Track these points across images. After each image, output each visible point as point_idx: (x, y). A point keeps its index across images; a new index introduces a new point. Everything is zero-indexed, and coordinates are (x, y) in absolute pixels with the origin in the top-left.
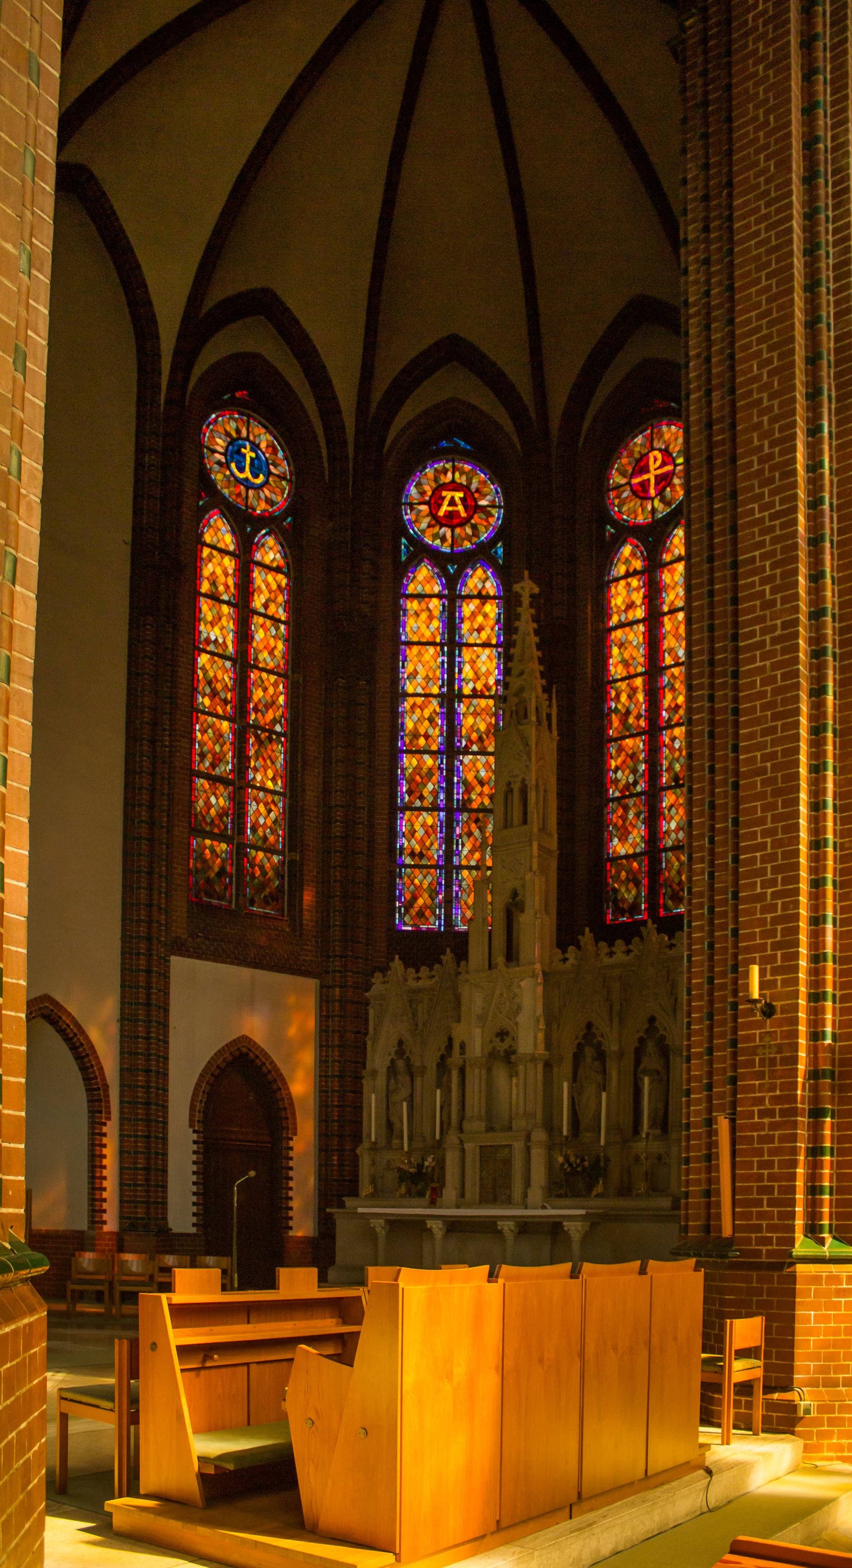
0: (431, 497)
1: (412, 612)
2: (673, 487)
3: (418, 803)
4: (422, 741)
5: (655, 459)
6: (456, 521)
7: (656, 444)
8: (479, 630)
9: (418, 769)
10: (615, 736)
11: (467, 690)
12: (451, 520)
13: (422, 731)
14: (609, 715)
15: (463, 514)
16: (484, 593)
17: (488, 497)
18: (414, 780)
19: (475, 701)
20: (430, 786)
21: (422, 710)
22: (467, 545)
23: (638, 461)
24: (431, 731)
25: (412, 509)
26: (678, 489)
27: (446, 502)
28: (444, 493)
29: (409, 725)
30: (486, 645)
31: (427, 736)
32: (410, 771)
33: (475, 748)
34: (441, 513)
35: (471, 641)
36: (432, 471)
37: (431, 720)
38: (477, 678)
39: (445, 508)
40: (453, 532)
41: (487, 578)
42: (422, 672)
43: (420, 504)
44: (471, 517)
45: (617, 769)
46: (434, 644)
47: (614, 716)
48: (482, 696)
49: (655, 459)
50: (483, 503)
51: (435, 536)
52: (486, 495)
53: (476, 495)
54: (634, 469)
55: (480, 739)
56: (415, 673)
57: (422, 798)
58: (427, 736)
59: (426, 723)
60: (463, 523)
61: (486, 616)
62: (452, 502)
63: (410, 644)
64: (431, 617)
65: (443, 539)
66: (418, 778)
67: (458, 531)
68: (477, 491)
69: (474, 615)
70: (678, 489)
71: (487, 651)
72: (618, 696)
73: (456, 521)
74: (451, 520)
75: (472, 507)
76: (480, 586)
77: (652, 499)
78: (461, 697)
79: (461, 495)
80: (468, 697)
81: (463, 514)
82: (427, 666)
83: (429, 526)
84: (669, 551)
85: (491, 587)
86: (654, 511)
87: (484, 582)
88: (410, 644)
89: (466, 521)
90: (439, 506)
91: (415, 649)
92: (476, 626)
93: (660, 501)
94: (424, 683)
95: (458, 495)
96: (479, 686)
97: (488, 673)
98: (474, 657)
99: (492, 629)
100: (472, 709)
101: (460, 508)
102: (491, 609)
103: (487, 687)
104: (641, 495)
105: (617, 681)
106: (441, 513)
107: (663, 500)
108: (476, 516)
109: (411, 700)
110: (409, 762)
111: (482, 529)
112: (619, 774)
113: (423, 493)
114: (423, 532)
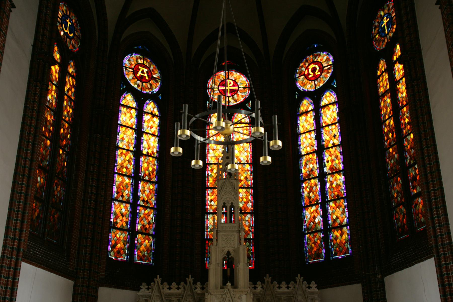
0: (134, 67)
1: (123, 112)
2: (238, 95)
3: (121, 198)
4: (124, 170)
5: (230, 83)
6: (144, 80)
7: (230, 77)
8: (151, 127)
9: (121, 183)
10: (211, 186)
11: (145, 152)
12: (141, 79)
13: (125, 165)
14: (208, 177)
15: (147, 78)
16: (153, 113)
17: (157, 74)
18: (120, 187)
19: (148, 158)
20: (127, 192)
21: (126, 156)
22: (148, 91)
23: (222, 81)
24: (129, 166)
25: (126, 69)
26: (240, 96)
27: (140, 71)
28: (140, 67)
29: (119, 161)
30: (153, 135)
31: (127, 168)
32: (118, 183)
33: (147, 178)
34: (138, 75)
35: (147, 131)
36: (135, 57)
37: (129, 161)
38: (149, 148)
39: (139, 74)
40: (142, 84)
41: (155, 108)
42: (126, 140)
43: (129, 68)
44: (150, 81)
45: (211, 201)
46: (132, 128)
47: (210, 178)
48: (151, 156)
49: (230, 83)
50: (155, 76)
51: (135, 83)
52: (156, 74)
53: (152, 72)
54: (220, 83)
55: (149, 174)
56: (123, 139)
57: (123, 196)
58: (127, 168)
59: (127, 162)
60: (147, 82)
61: (154, 122)
62: (143, 72)
63: (122, 126)
64: (131, 117)
65: (138, 86)
66: (121, 187)
67: (144, 84)
68: (153, 71)
69: (149, 121)
70: (240, 96)
71: (153, 138)
72: (212, 170)
73: (144, 80)
74: (141, 79)
75: (151, 78)
76: (152, 110)
77: (229, 97)
78: (142, 155)
79: (147, 70)
80: (145, 155)
81: (147, 78)
82: (128, 137)
83: (133, 78)
84: (236, 118)
85: (156, 112)
86: (229, 102)
87: (154, 109)
88: (122, 126)
89: (148, 81)
90: (137, 73)
91: (124, 129)
92: (150, 126)
93: (232, 98)
94: (127, 144)
95: (145, 70)
96: (150, 151)
97: (154, 147)
98: (148, 138)
99: (156, 129)
100: (146, 161)
101: (146, 75)
102: (156, 120)
103: (153, 152)
104: (223, 94)
105: (212, 164)
106: (138, 75)
107: (233, 98)
108: (152, 81)
109: (121, 151)
110: (118, 179)
111: (154, 87)
112: (213, 203)
113: (131, 64)
114: (130, 80)
